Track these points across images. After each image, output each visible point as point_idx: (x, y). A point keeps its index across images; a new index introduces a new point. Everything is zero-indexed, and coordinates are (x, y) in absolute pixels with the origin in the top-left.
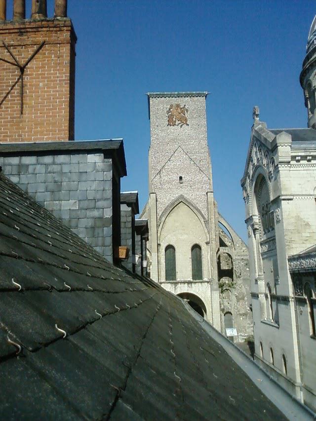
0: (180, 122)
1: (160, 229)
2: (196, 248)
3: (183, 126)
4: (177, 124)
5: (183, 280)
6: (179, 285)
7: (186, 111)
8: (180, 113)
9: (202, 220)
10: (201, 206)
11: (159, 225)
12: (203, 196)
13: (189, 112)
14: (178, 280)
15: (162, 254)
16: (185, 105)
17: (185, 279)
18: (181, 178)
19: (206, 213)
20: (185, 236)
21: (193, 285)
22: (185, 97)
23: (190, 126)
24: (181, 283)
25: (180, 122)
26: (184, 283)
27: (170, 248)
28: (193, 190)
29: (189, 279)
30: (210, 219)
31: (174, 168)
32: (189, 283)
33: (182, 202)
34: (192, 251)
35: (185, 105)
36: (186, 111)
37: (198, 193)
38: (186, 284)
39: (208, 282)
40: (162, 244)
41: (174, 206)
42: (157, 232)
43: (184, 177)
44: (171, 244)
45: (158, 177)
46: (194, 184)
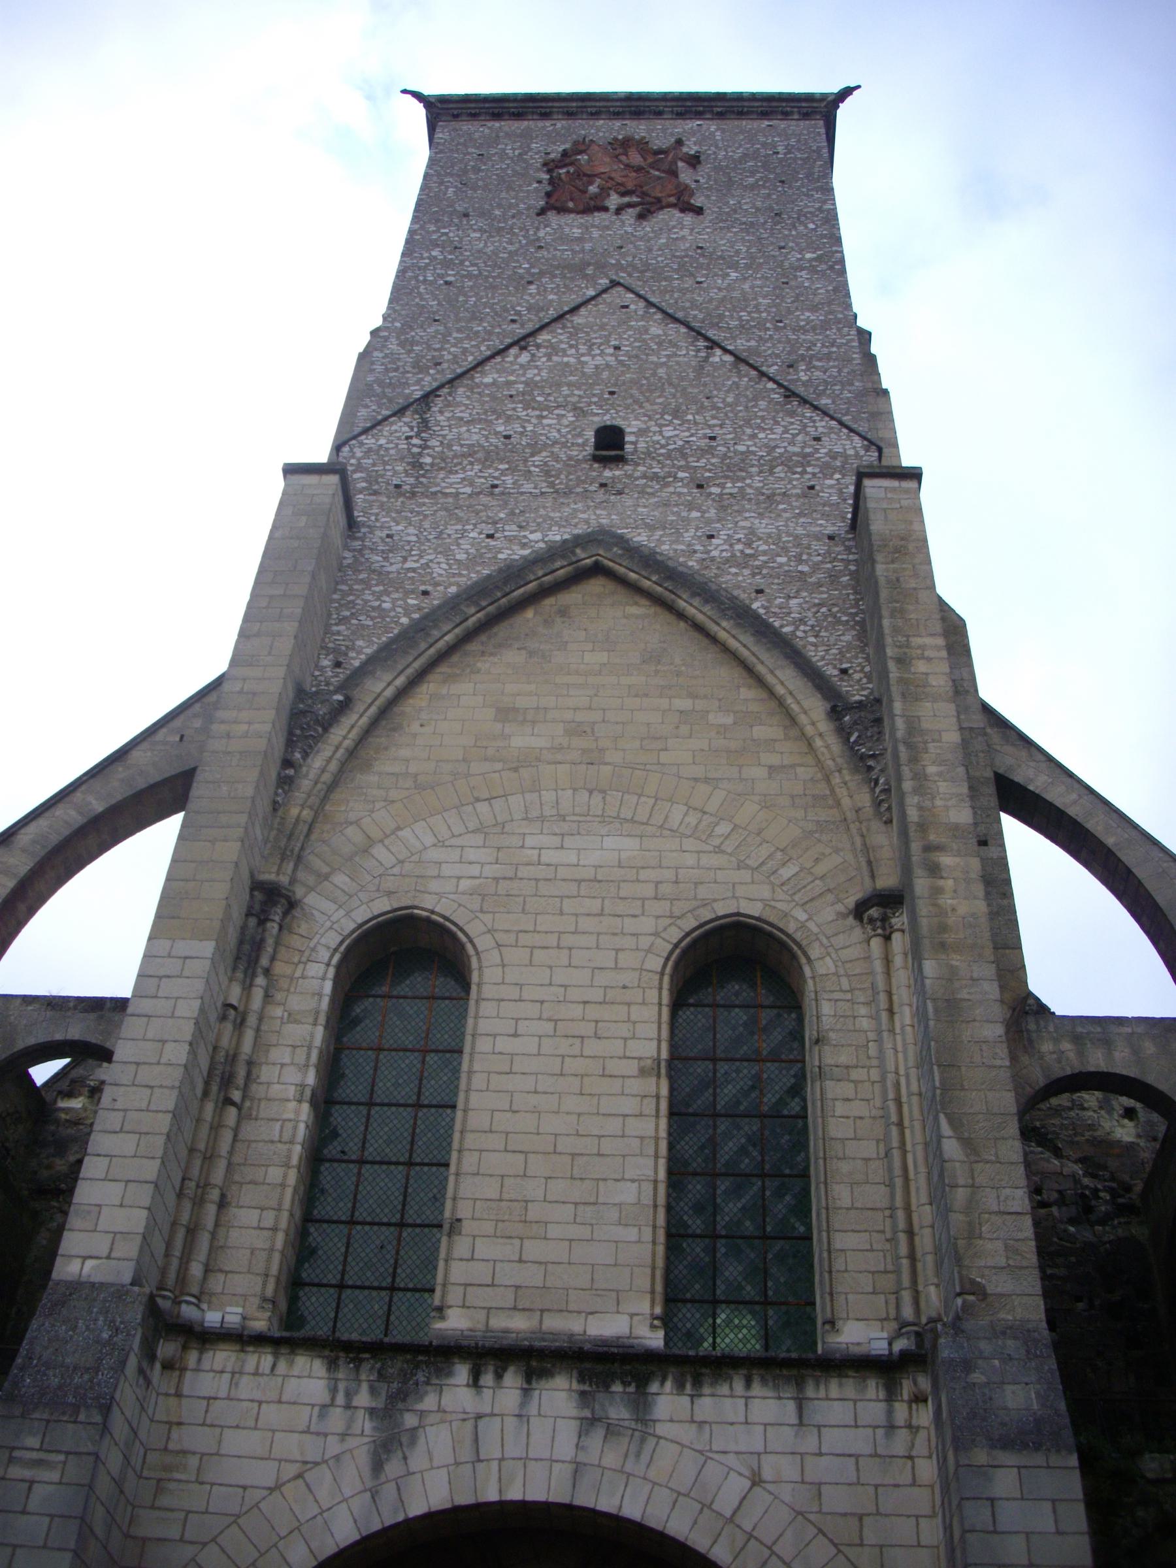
0: (635, 199)
1: (320, 762)
2: (732, 970)
3: (662, 216)
4: (613, 207)
5: (519, 1325)
6: (456, 1392)
7: (680, 164)
8: (639, 169)
9: (813, 709)
10: (789, 611)
11: (327, 724)
12: (819, 547)
13: (705, 169)
14: (456, 1322)
15: (296, 1003)
16: (679, 142)
17: (555, 1323)
18: (609, 444)
19: (856, 662)
20: (609, 848)
21: (668, 1401)
22: (681, 115)
23: (709, 216)
24: (491, 1356)
25: (626, 199)
26: (533, 1359)
27: (410, 957)
28: (723, 508)
29: (609, 1326)
30: (902, 661)
31: (559, 385)
32: (606, 1368)
33: (596, 563)
34: (678, 1004)
35: (679, 142)
36: (680, 164)
37: (763, 527)
38: (558, 1395)
39: (886, 1369)
40: (312, 900)
41: (503, 602)
42: (286, 783)
43: (642, 432)
44: (440, 899)
45: (401, 427)
46: (735, 467)
